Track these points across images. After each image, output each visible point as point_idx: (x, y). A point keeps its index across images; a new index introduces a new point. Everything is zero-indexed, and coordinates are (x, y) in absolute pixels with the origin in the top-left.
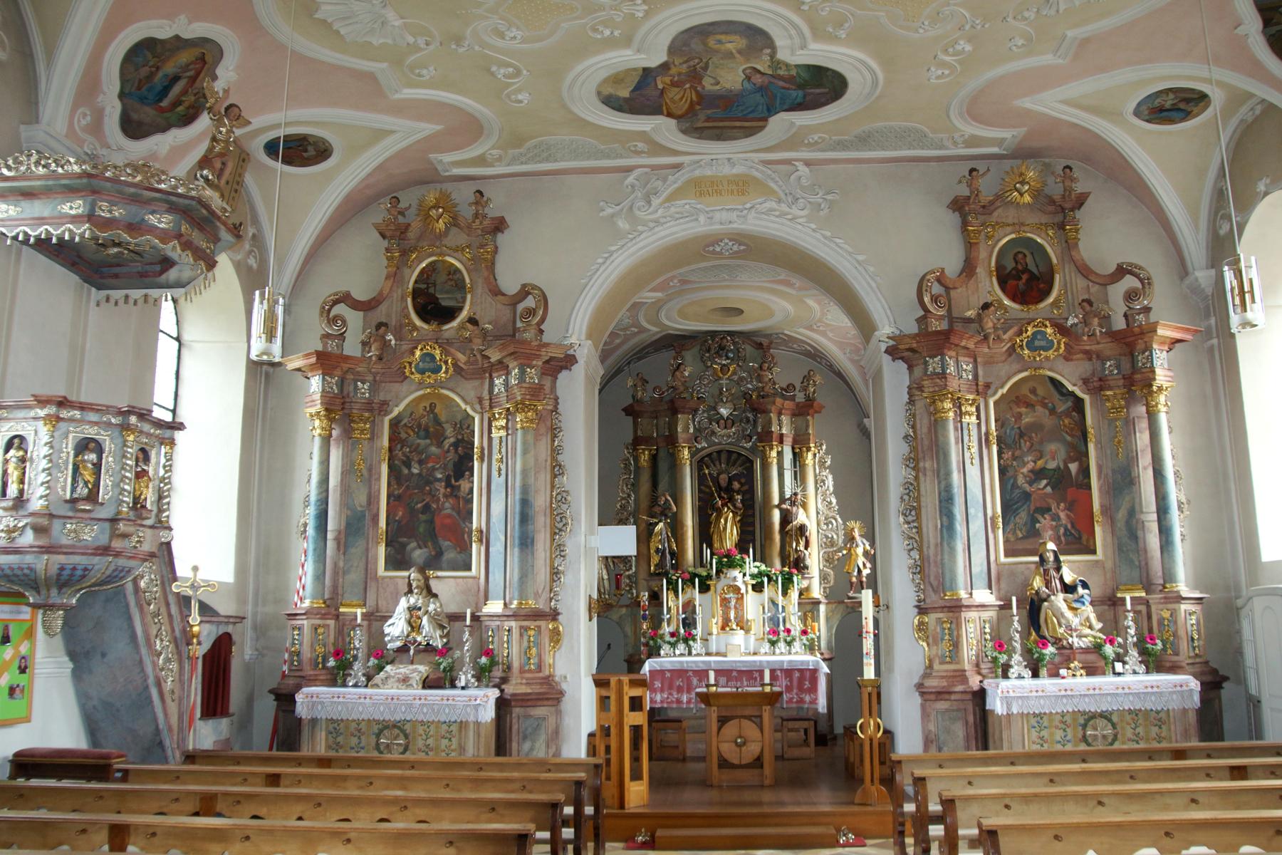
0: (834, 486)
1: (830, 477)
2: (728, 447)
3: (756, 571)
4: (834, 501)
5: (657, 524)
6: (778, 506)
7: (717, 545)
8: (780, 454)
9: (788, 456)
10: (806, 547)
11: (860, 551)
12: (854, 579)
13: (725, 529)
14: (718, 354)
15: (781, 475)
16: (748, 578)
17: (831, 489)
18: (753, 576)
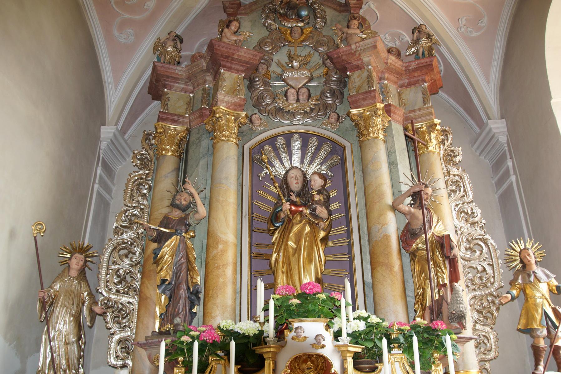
0: (473, 189)
1: (466, 177)
2: (301, 129)
3: (361, 326)
4: (478, 212)
5: (170, 236)
6: (394, 208)
7: (281, 280)
8: (387, 130)
9: (400, 143)
10: (454, 277)
11: (543, 288)
12: (542, 343)
13: (297, 251)
14: (285, 17)
15: (392, 164)
16: (344, 339)
17: (470, 194)
18: (355, 337)
